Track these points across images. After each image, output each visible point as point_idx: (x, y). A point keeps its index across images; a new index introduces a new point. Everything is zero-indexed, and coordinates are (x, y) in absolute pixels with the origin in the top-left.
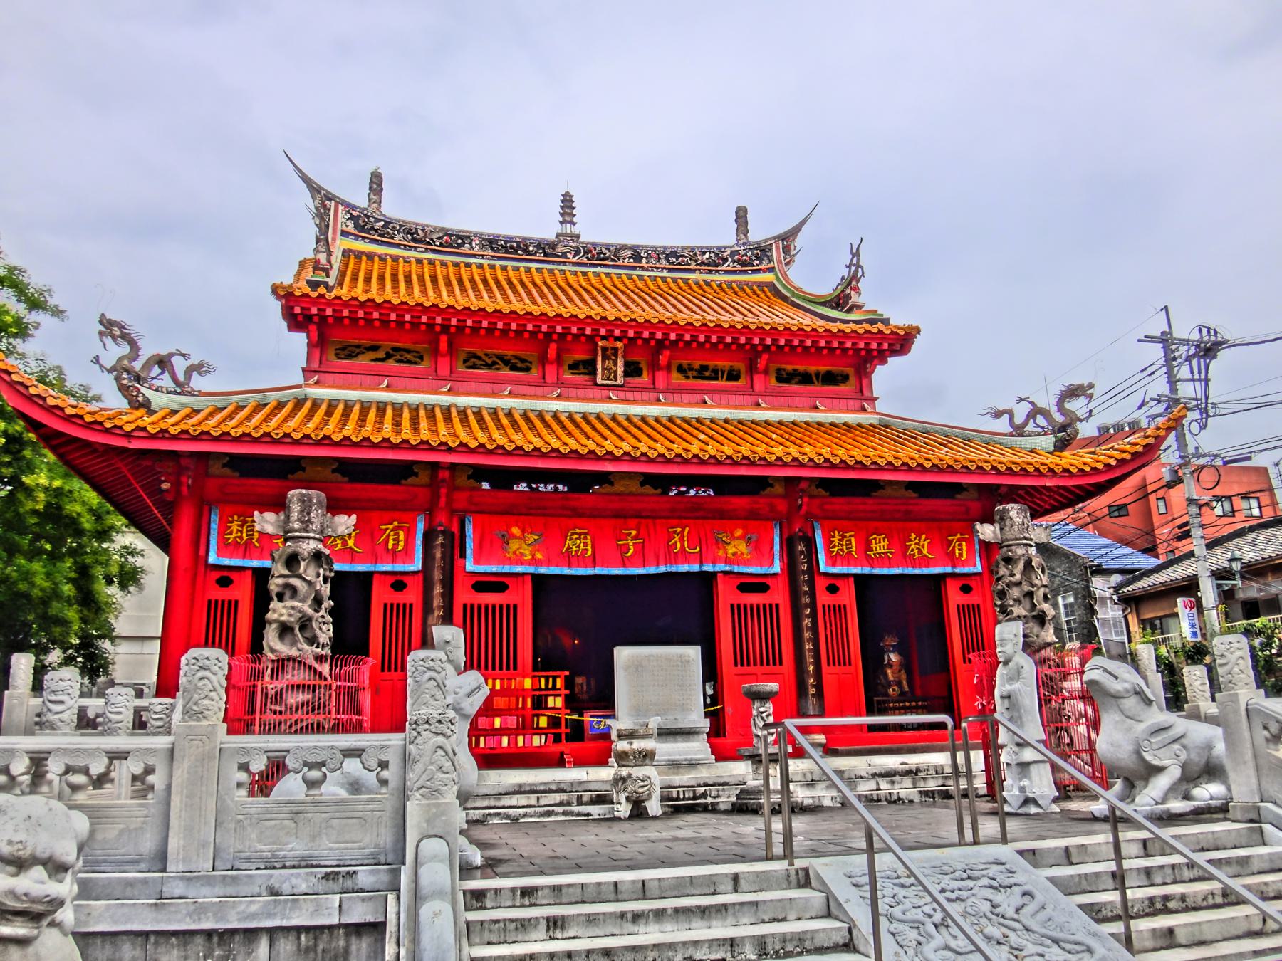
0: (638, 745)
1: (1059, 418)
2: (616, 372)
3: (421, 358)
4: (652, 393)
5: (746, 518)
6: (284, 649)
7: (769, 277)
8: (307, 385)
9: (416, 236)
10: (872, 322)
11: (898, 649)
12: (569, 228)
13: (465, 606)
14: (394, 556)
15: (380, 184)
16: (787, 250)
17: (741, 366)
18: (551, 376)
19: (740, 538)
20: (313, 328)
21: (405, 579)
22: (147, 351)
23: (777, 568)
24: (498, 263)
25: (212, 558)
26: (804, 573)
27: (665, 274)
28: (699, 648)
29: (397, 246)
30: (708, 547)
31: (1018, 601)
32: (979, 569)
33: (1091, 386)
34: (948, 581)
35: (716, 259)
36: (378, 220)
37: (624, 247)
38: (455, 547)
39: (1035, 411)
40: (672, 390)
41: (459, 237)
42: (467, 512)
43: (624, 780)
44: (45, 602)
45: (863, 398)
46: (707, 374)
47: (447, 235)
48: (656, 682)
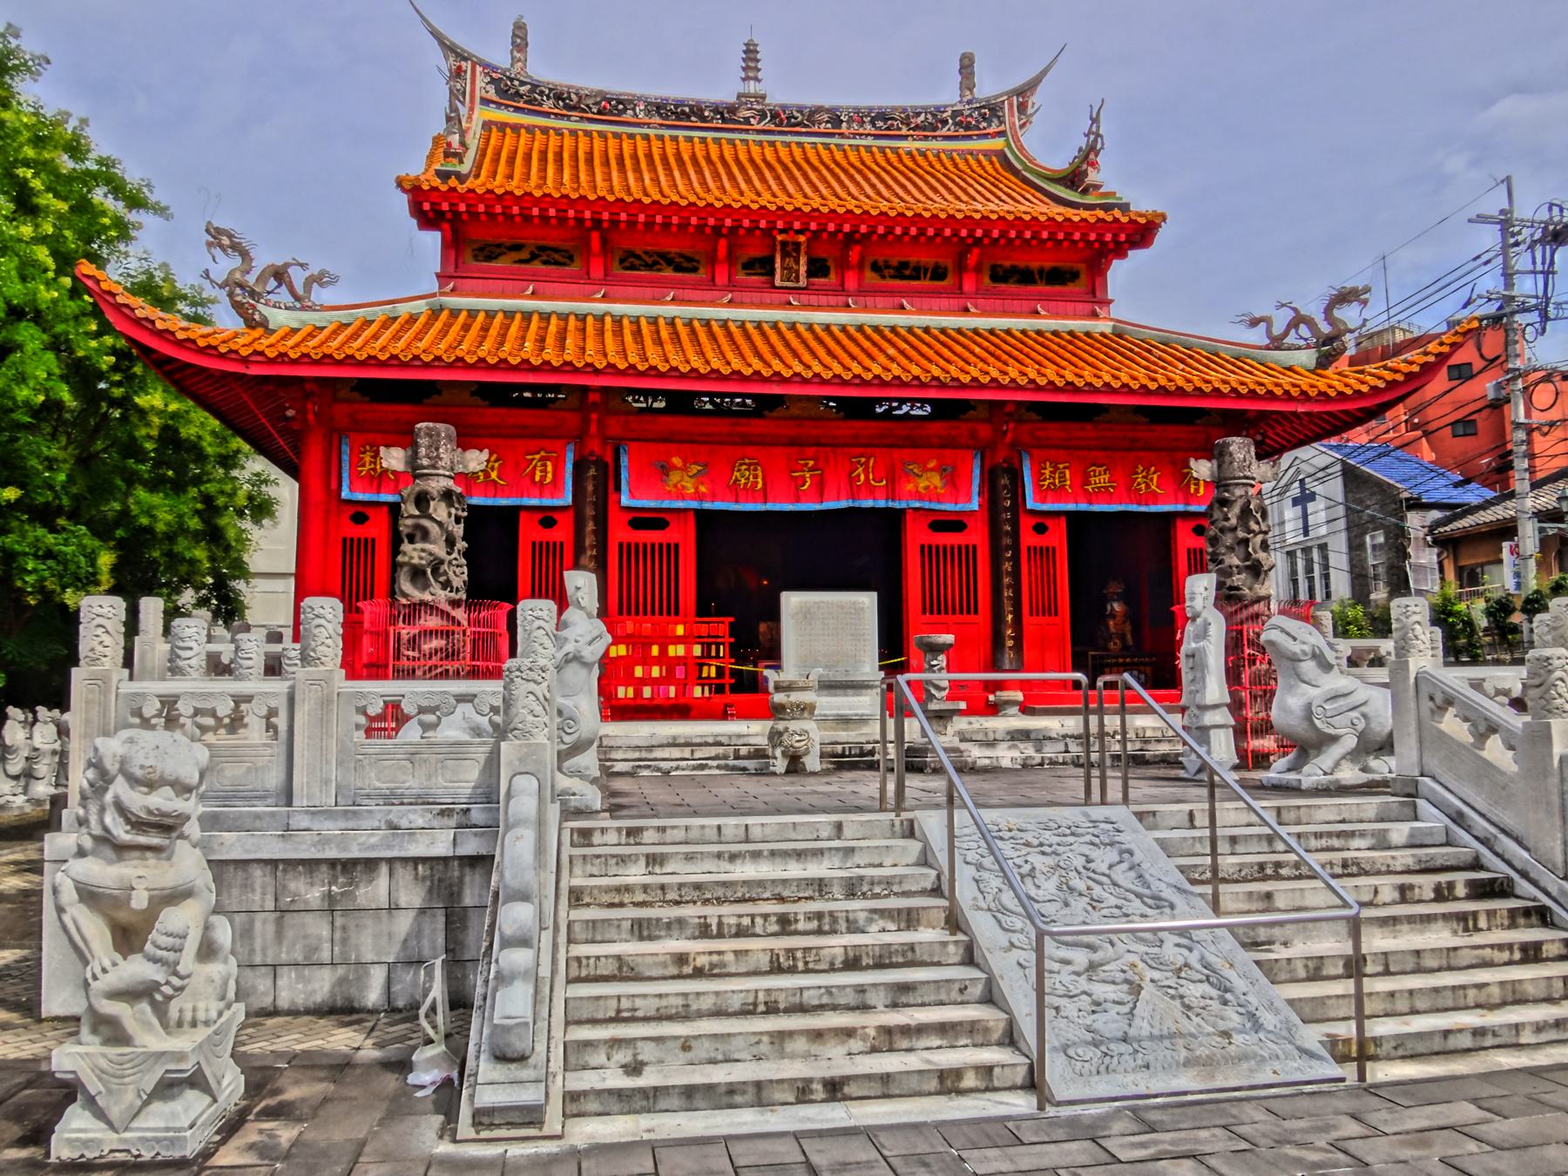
0: (795, 697)
1: (1325, 328)
2: (797, 272)
3: (571, 258)
4: (840, 296)
5: (942, 446)
6: (417, 595)
7: (998, 143)
8: (442, 294)
9: (567, 102)
10: (1107, 208)
11: (1125, 599)
12: (752, 87)
13: (621, 545)
14: (541, 488)
15: (524, 39)
16: (1022, 108)
17: (948, 263)
18: (721, 279)
19: (932, 470)
20: (446, 226)
21: (556, 516)
22: (263, 259)
23: (974, 505)
24: (667, 133)
25: (345, 494)
26: (1006, 510)
27: (869, 141)
28: (875, 594)
29: (547, 115)
31: (1231, 549)
33: (1367, 290)
34: (1179, 523)
35: (932, 123)
36: (523, 83)
37: (819, 109)
38: (608, 481)
39: (1298, 320)
40: (863, 291)
41: (619, 102)
42: (623, 439)
43: (780, 734)
45: (1095, 299)
46: (907, 272)
47: (605, 99)
48: (827, 629)
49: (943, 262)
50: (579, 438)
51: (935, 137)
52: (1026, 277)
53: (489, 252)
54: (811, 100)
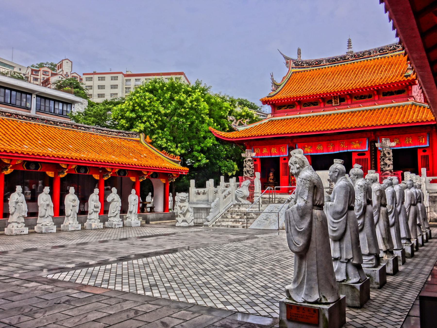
3: (294, 107)
9: (309, 64)
19: (358, 143)
23: (367, 149)
26: (373, 150)
27: (379, 56)
29: (305, 68)
30: (349, 145)
32: (428, 145)
37: (366, 51)
40: (352, 103)
41: (320, 61)
47: (317, 61)
49: (371, 94)
50: (289, 144)
51: (396, 51)
52: (391, 94)
53: (280, 107)
54: (363, 50)
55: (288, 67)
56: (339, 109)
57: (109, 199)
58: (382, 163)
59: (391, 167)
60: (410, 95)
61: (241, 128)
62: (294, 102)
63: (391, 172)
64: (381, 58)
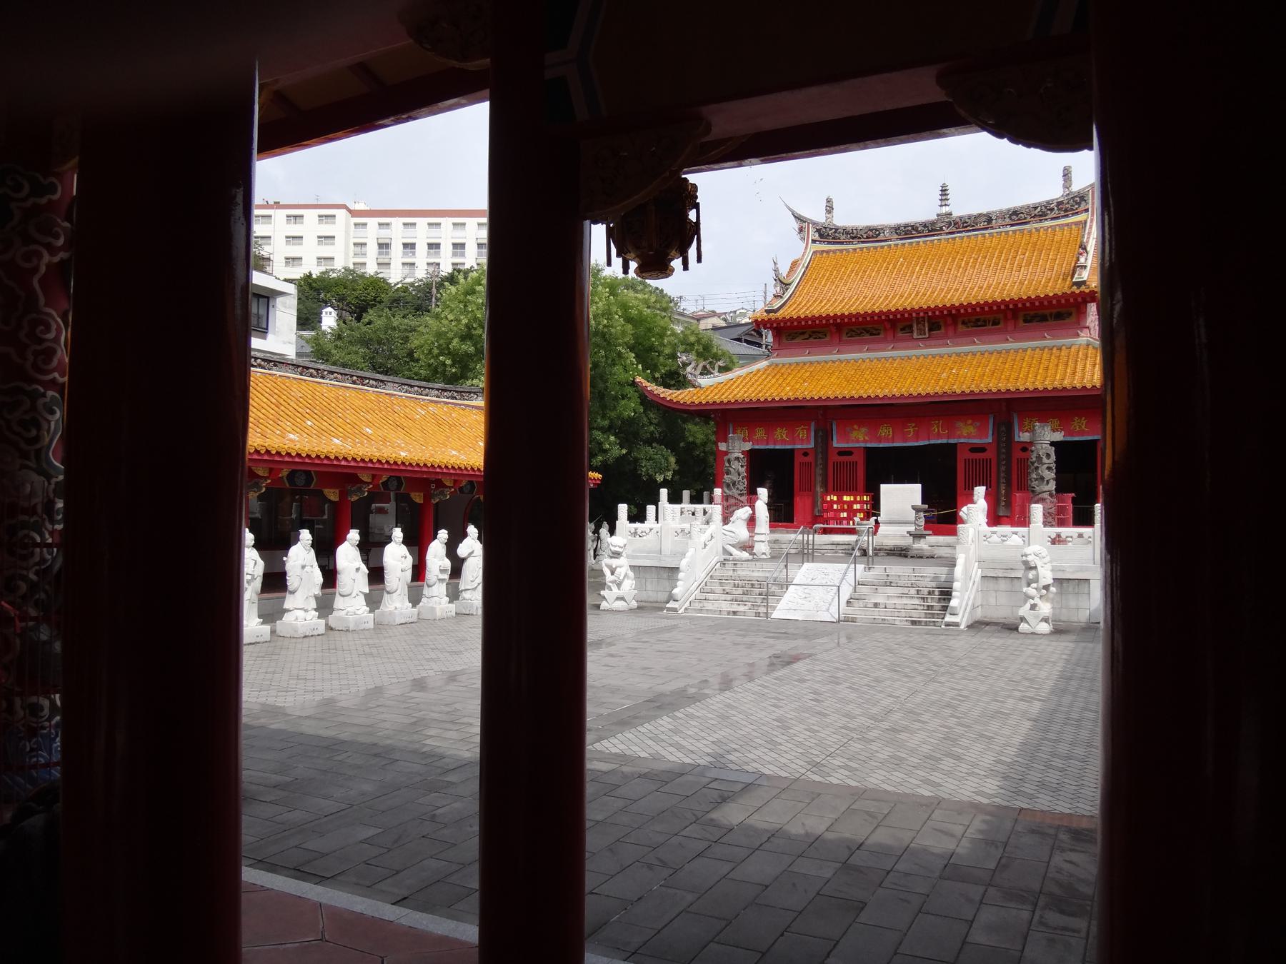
9: (853, 235)
12: (945, 210)
14: (802, 441)
17: (1001, 316)
23: (990, 440)
27: (1009, 228)
29: (842, 243)
35: (1042, 212)
37: (980, 215)
44: (704, 444)
52: (1044, 318)
54: (975, 212)
55: (803, 239)
56: (927, 347)
57: (462, 550)
58: (1034, 476)
59: (1052, 486)
60: (1082, 324)
61: (704, 381)
62: (828, 325)
63: (1051, 495)
64: (1014, 232)
